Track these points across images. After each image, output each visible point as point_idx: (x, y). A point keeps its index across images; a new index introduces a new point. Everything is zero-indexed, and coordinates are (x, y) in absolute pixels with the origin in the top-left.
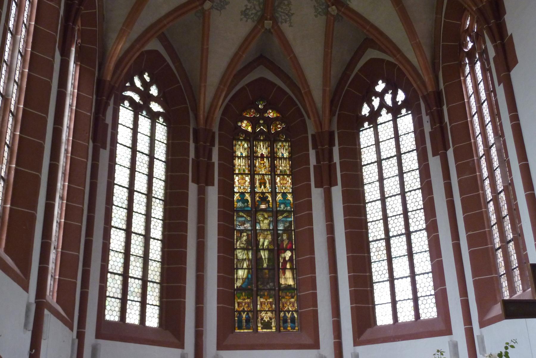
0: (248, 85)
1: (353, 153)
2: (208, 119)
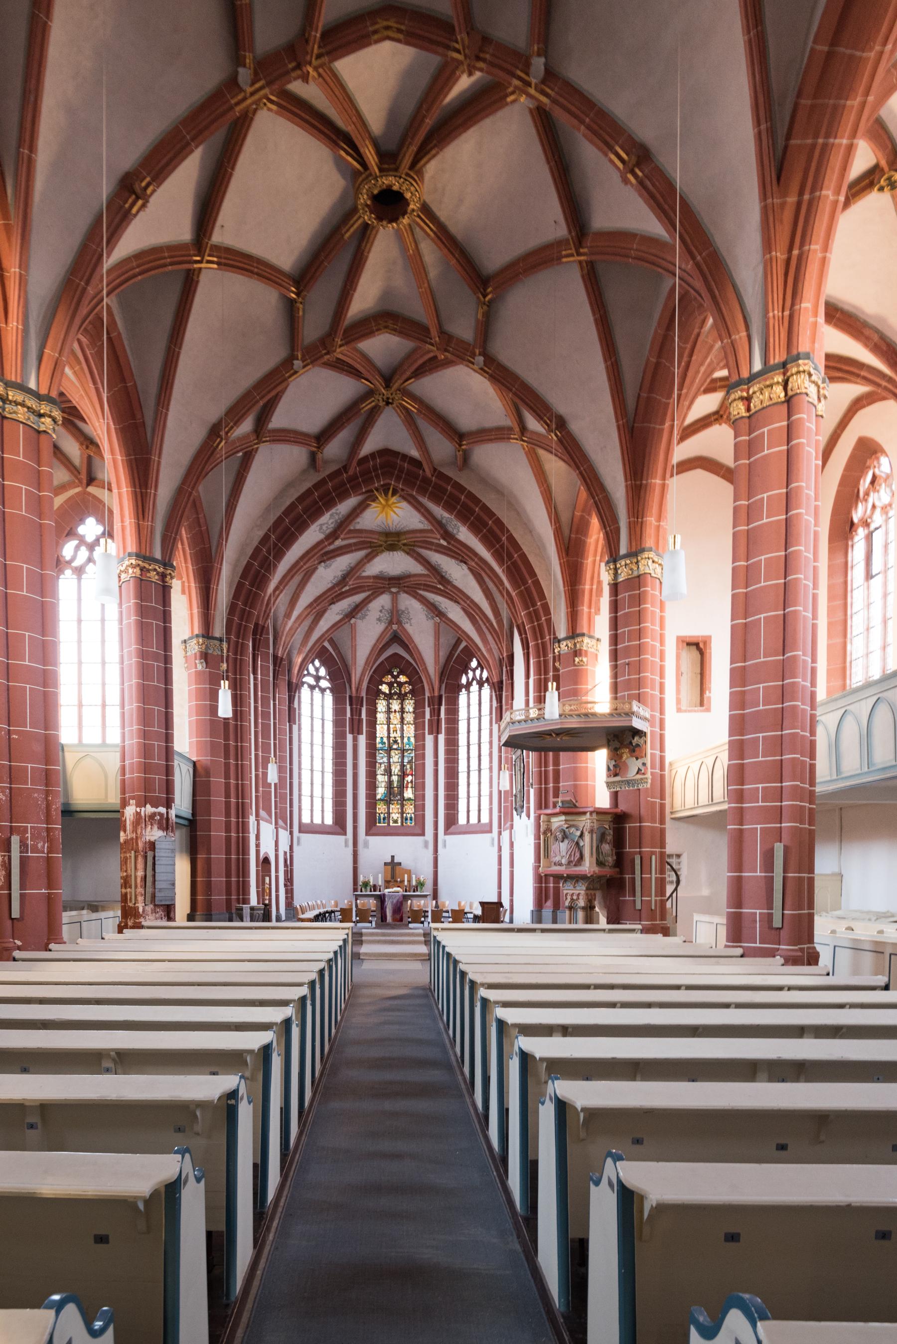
0: (386, 659)
1: (453, 712)
2: (358, 689)
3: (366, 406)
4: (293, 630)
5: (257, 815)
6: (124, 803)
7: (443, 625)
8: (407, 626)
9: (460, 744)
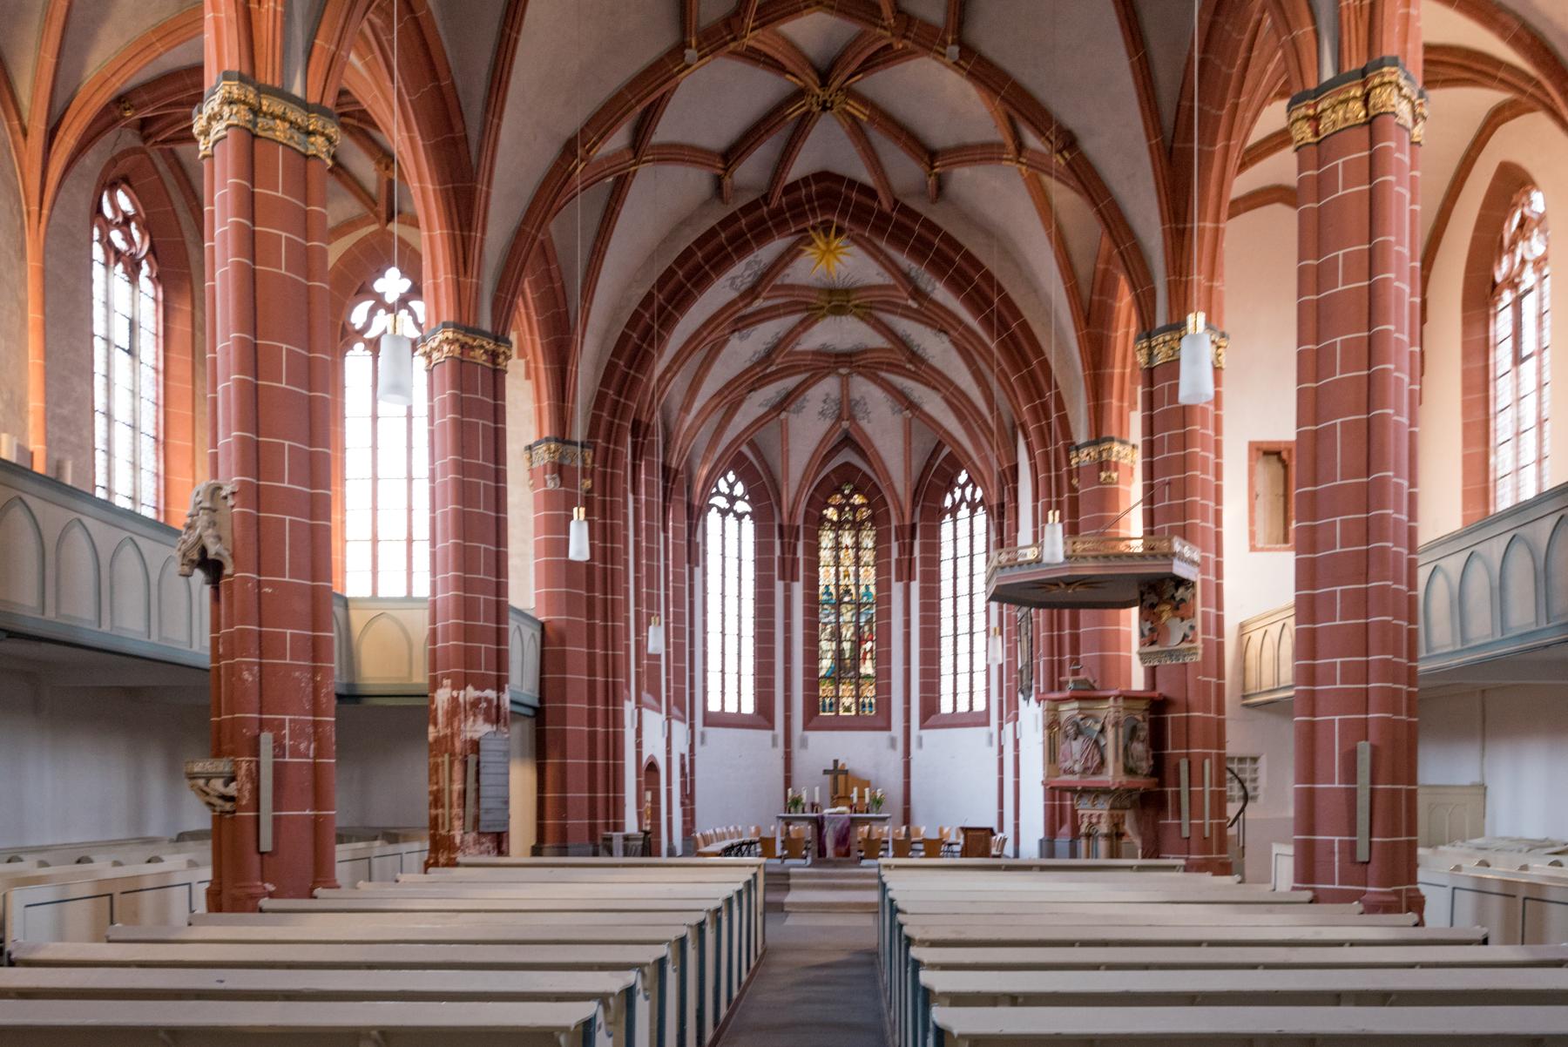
1: (933, 548)
3: (794, 112)
4: (694, 430)
5: (638, 700)
6: (435, 684)
7: (916, 423)
8: (863, 423)
9: (943, 595)
